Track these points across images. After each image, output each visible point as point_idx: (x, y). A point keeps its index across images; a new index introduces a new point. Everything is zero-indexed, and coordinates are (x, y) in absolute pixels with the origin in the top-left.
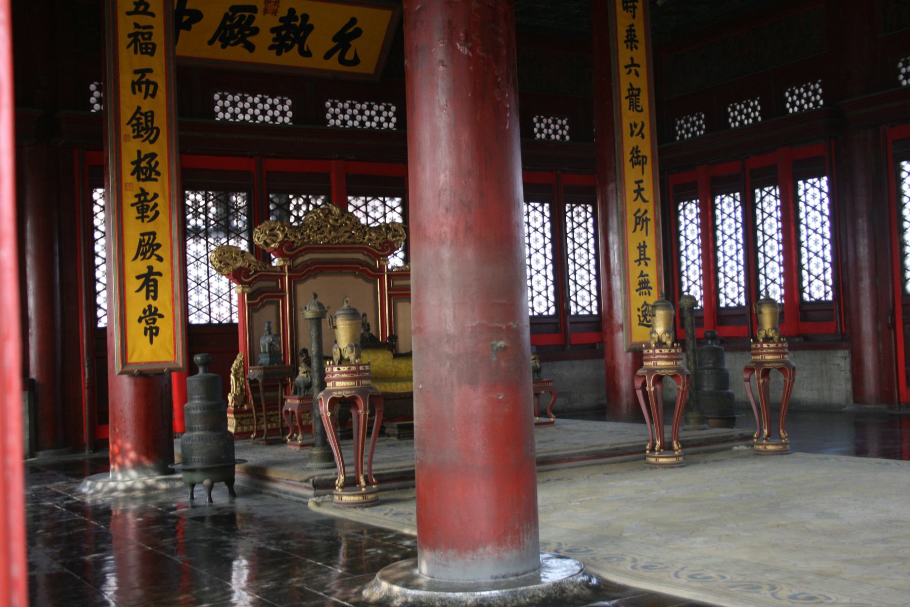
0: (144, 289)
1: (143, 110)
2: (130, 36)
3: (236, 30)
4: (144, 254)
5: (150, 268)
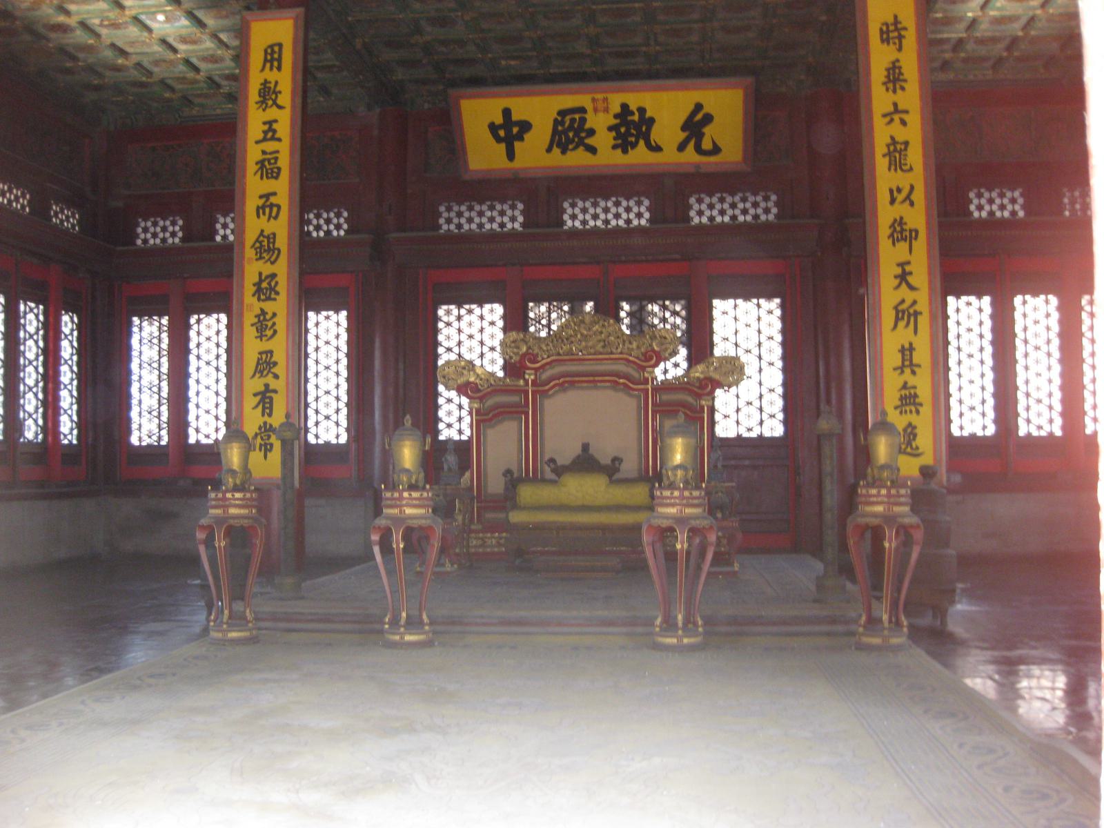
0: (260, 407)
1: (266, 233)
2: (257, 163)
3: (571, 134)
4: (261, 372)
5: (267, 386)
